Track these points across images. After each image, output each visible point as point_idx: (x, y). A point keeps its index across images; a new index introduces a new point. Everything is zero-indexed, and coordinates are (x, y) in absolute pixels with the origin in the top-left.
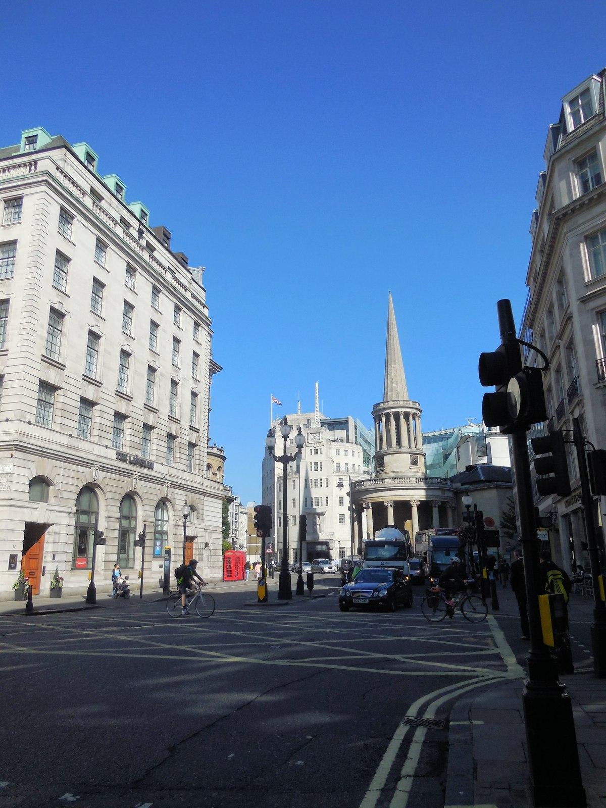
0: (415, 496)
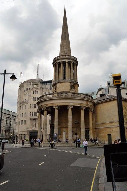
0: (70, 103)
